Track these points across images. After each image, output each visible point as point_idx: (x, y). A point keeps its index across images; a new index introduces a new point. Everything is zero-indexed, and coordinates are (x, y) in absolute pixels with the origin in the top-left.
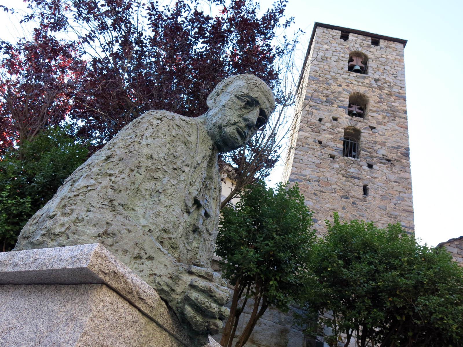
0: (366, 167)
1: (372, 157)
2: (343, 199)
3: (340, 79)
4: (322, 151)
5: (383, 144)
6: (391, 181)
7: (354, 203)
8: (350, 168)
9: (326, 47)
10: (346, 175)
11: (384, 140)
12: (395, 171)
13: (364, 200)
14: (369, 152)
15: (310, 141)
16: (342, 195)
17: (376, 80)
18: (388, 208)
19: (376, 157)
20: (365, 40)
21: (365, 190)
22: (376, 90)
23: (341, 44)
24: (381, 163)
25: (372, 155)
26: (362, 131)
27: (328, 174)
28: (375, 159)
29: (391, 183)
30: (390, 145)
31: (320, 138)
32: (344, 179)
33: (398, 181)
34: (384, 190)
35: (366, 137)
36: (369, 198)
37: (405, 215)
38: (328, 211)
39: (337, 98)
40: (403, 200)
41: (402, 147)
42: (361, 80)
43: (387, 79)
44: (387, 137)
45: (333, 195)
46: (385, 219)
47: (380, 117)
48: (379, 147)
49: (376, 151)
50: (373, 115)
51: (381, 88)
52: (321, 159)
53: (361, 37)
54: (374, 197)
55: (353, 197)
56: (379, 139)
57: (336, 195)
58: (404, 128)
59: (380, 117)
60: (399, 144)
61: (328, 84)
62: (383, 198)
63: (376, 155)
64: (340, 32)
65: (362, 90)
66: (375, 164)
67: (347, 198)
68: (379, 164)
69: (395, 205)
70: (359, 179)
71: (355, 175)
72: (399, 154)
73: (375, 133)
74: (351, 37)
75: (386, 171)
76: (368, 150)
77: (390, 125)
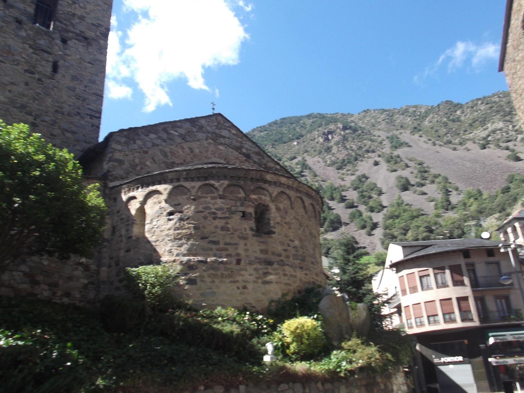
0: (58, 42)
1: (68, 31)
2: (27, 74)
4: (6, 11)
5: (82, 18)
6: (84, 61)
7: (39, 80)
8: (40, 39)
10: (34, 47)
11: (84, 15)
12: (90, 50)
13: (51, 78)
14: (65, 25)
16: (26, 68)
18: (77, 90)
19: (72, 32)
21: (55, 68)
24: (76, 40)
25: (68, 28)
27: (10, 42)
28: (71, 34)
29: (85, 64)
30: (90, 21)
32: (31, 50)
33: (92, 62)
34: (75, 70)
36: (58, 76)
37: (94, 98)
38: (6, 85)
40: (94, 82)
41: (102, 26)
44: (87, 11)
45: (15, 67)
46: (73, 101)
48: (77, 21)
49: (73, 25)
52: (4, 21)
54: (64, 76)
55: (39, 73)
56: (79, 12)
57: (18, 68)
58: (108, 5)
60: (100, 22)
62: (74, 78)
63: (72, 29)
66: (70, 39)
67: (32, 73)
68: (74, 41)
69: (86, 87)
70: (49, 53)
71: (45, 48)
72: (98, 33)
73: (75, 3)
75: (81, 49)
76: (64, 22)
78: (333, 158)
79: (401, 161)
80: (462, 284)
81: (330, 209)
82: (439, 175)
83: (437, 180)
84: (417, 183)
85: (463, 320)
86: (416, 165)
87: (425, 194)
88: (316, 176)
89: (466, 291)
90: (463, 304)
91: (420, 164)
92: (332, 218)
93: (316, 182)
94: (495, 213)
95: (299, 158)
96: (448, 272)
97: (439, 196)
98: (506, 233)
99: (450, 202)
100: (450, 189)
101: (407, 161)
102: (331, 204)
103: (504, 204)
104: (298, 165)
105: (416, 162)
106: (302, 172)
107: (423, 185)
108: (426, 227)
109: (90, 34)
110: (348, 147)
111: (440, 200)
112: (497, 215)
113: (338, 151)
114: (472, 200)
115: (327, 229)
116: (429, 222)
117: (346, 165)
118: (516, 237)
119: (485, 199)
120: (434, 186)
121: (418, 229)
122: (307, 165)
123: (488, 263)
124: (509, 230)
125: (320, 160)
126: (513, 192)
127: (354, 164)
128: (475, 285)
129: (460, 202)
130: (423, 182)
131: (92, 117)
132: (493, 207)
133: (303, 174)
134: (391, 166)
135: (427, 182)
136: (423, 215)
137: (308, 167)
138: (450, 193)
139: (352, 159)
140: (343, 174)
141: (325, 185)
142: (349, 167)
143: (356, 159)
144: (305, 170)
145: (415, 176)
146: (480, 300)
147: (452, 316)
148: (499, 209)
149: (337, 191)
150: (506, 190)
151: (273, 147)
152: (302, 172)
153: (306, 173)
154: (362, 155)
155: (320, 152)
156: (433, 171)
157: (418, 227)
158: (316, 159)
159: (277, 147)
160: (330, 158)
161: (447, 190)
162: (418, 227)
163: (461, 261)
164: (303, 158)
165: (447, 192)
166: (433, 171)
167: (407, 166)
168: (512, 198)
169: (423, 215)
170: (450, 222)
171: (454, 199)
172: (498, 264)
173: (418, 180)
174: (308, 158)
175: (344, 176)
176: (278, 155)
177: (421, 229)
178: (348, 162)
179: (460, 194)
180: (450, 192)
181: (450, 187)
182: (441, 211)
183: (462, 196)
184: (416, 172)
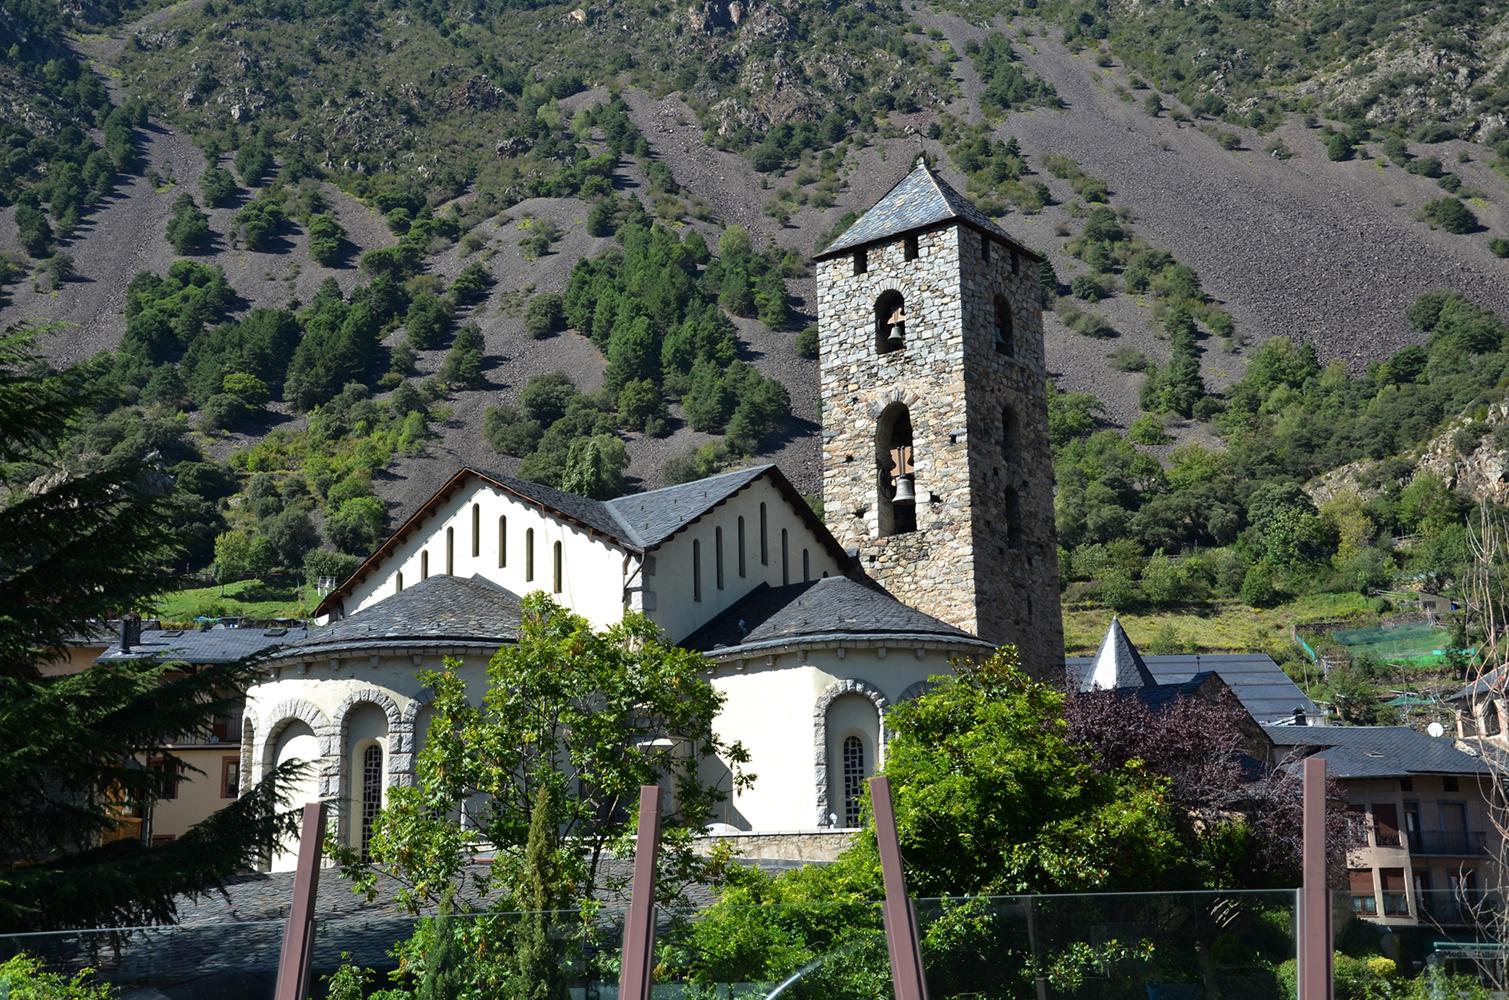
1: (1030, 544)
3: (992, 376)
15: (982, 522)
17: (1022, 370)
20: (1003, 259)
23: (984, 275)
26: (1020, 493)
31: (991, 518)
35: (1025, 507)
39: (992, 421)
42: (1008, 373)
43: (1032, 366)
51: (1026, 390)
61: (983, 388)
65: (1011, 395)
70: (1023, 587)
77: (1040, 474)
78: (743, 115)
79: (1025, 171)
80: (1394, 843)
81: (744, 353)
82: (1168, 259)
83: (1157, 281)
84: (1082, 281)
85: (1388, 913)
86: (1081, 199)
87: (1111, 334)
88: (673, 188)
89: (1400, 858)
90: (1391, 881)
91: (1095, 198)
92: (758, 399)
93: (678, 218)
94: (1359, 457)
95: (596, 95)
96: (1369, 816)
97: (1166, 355)
98: (1468, 712)
99: (1201, 387)
100: (1203, 327)
101: (1046, 177)
102: (748, 329)
103: (1397, 426)
104: (594, 123)
105: (1080, 183)
106: (616, 163)
107: (1102, 294)
108: (1111, 483)
110: (809, 72)
111: (1164, 374)
112: (1365, 466)
113: (769, 83)
114: (1282, 391)
115: (738, 442)
116: (1125, 465)
117: (796, 154)
118: (1493, 728)
119: (1327, 392)
120: (1145, 304)
121: (1084, 487)
122: (636, 135)
123: (1444, 804)
124: (1479, 709)
125: (690, 114)
126: (1434, 381)
127: (829, 156)
128: (1416, 846)
129: (1237, 389)
130: (1103, 279)
132: (1356, 434)
133: (619, 172)
134: (985, 188)
135: (1120, 280)
136: (1100, 424)
137: (640, 143)
138: (1200, 343)
139: (824, 132)
140: (786, 196)
141: (719, 244)
142: (809, 164)
143: (839, 133)
144: (625, 157)
145: (1073, 248)
146: (1422, 875)
147: (1369, 903)
148: (1375, 443)
149: (768, 276)
150: (1406, 371)
151: (478, 19)
152: (616, 163)
153: (633, 168)
154: (865, 118)
155: (689, 80)
156: (1148, 237)
157: (1084, 478)
158: (671, 105)
159: (496, 20)
160: (731, 113)
161: (1192, 329)
162: (1084, 478)
163: (1398, 798)
164: (615, 97)
165: (1193, 342)
166: (1148, 237)
167: (1047, 200)
168: (1426, 407)
169: (1100, 424)
170: (1198, 471)
171: (1220, 372)
172: (1462, 806)
173: (1086, 270)
174: (633, 95)
175: (791, 207)
176: (502, 60)
177: (1095, 488)
178: (807, 143)
179: (1236, 352)
180: (1204, 336)
181: (1205, 317)
182: (1165, 418)
183: (1245, 360)
184: (1078, 229)
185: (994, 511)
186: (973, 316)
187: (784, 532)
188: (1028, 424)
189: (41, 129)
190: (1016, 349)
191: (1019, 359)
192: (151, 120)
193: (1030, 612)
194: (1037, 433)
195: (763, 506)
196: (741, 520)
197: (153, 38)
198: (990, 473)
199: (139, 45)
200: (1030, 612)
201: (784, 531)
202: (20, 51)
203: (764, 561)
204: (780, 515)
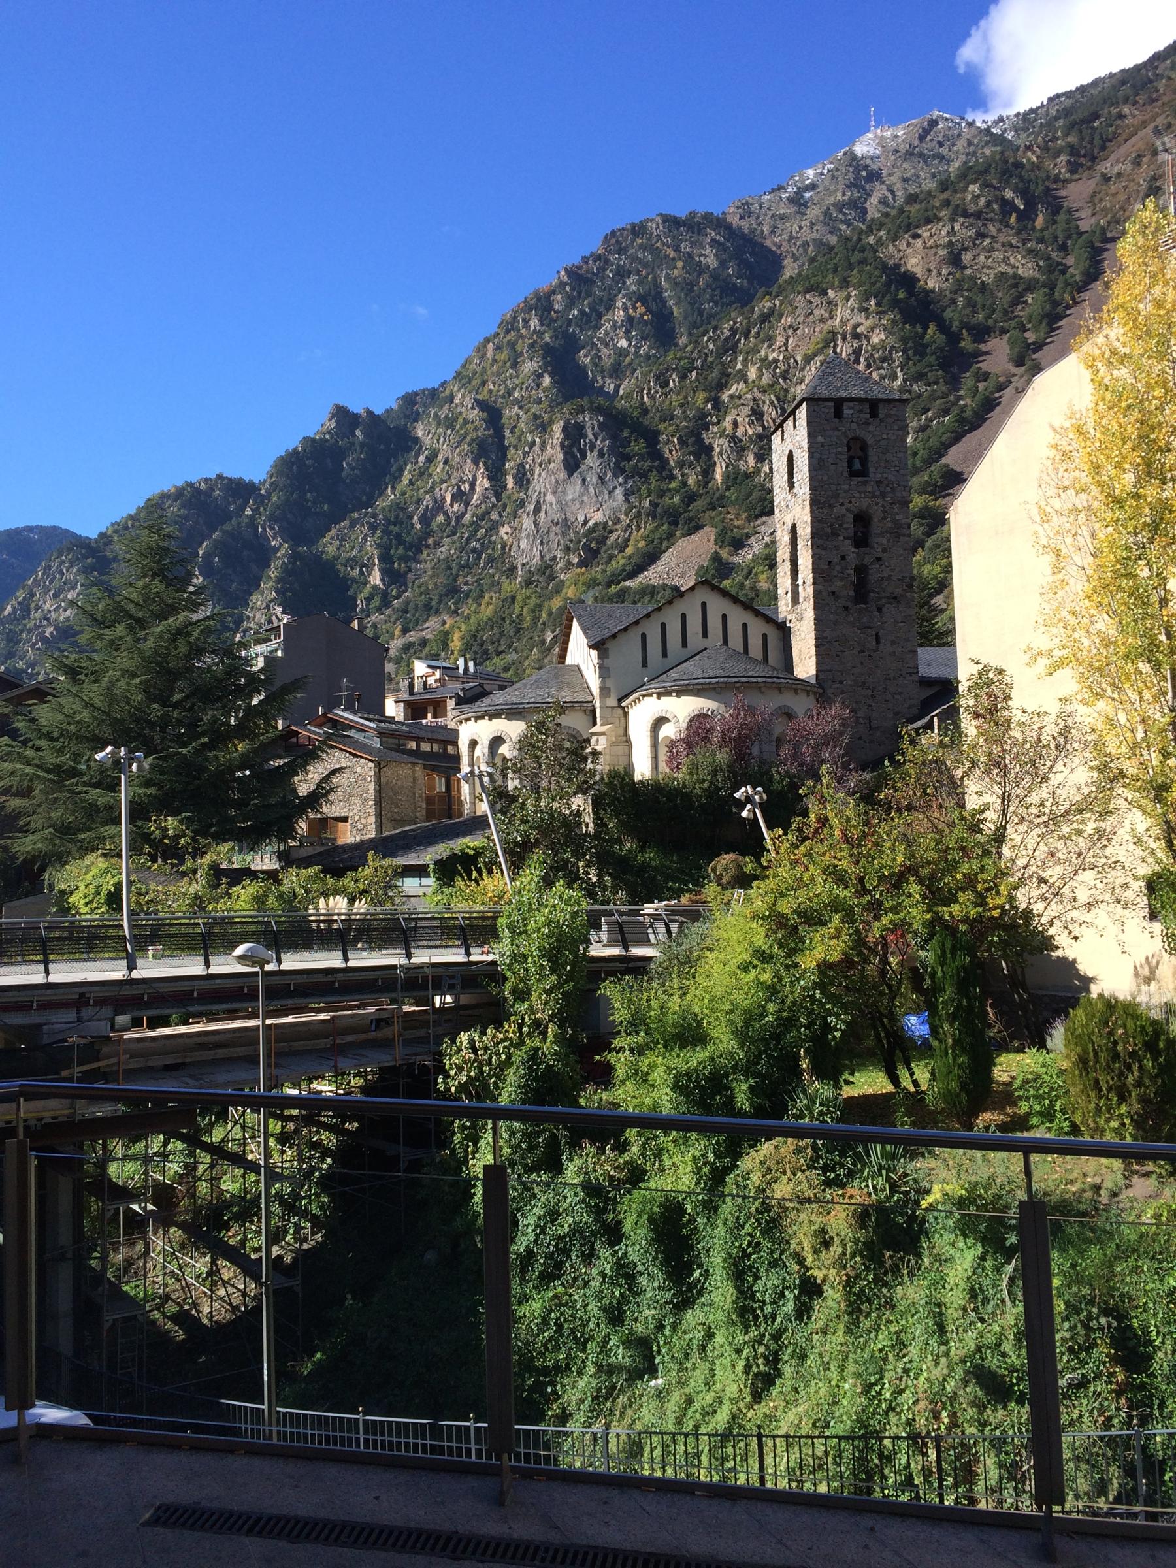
5: (889, 578)
9: (820, 439)
17: (879, 483)
20: (860, 411)
22: (880, 500)
23: (836, 429)
31: (833, 589)
35: (874, 574)
42: (862, 488)
43: (892, 477)
47: (885, 541)
50: (879, 541)
53: (858, 406)
59: (885, 541)
62: (893, 643)
64: (831, 404)
65: (865, 503)
74: (847, 411)
109: (899, 591)
131: (911, 674)
185: (839, 584)
186: (821, 460)
187: (724, 617)
188: (884, 518)
189: (1026, 269)
190: (871, 470)
191: (874, 474)
192: (1109, 235)
193: (878, 642)
194: (894, 521)
195: (704, 605)
196: (683, 616)
197: (1116, 170)
198: (836, 560)
199: (1106, 179)
200: (878, 642)
201: (724, 617)
202: (1019, 219)
203: (705, 634)
204: (717, 606)
